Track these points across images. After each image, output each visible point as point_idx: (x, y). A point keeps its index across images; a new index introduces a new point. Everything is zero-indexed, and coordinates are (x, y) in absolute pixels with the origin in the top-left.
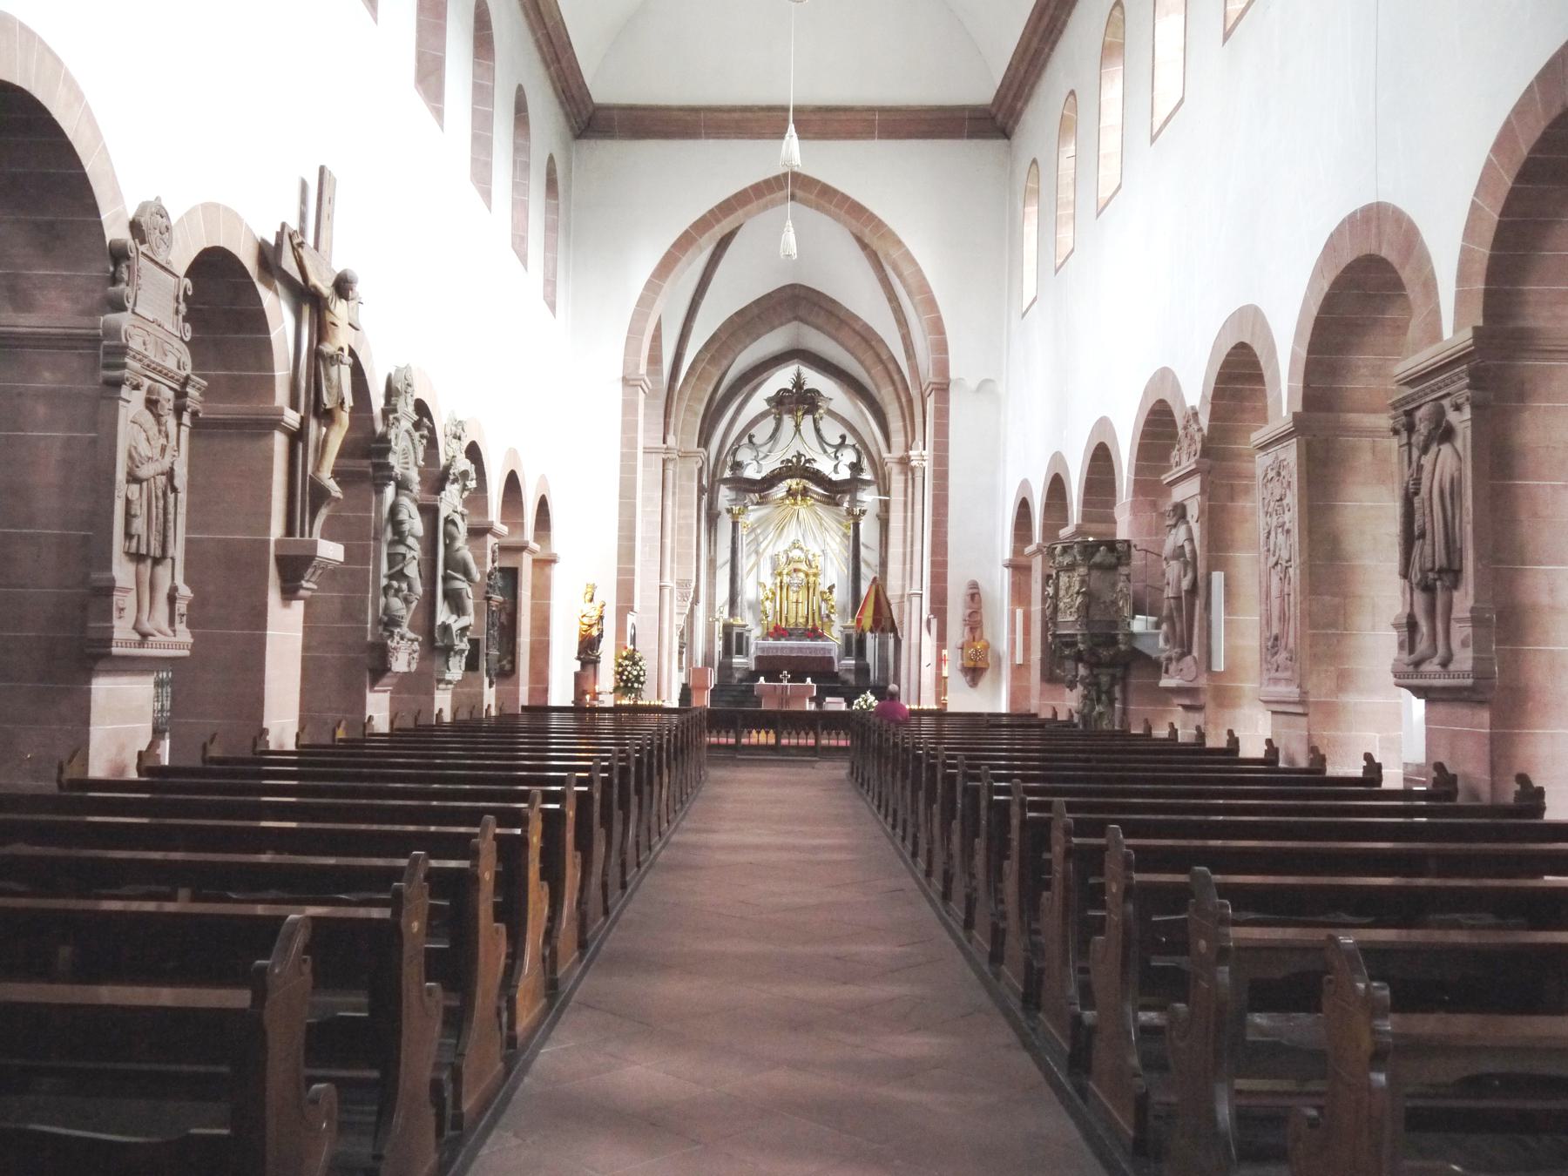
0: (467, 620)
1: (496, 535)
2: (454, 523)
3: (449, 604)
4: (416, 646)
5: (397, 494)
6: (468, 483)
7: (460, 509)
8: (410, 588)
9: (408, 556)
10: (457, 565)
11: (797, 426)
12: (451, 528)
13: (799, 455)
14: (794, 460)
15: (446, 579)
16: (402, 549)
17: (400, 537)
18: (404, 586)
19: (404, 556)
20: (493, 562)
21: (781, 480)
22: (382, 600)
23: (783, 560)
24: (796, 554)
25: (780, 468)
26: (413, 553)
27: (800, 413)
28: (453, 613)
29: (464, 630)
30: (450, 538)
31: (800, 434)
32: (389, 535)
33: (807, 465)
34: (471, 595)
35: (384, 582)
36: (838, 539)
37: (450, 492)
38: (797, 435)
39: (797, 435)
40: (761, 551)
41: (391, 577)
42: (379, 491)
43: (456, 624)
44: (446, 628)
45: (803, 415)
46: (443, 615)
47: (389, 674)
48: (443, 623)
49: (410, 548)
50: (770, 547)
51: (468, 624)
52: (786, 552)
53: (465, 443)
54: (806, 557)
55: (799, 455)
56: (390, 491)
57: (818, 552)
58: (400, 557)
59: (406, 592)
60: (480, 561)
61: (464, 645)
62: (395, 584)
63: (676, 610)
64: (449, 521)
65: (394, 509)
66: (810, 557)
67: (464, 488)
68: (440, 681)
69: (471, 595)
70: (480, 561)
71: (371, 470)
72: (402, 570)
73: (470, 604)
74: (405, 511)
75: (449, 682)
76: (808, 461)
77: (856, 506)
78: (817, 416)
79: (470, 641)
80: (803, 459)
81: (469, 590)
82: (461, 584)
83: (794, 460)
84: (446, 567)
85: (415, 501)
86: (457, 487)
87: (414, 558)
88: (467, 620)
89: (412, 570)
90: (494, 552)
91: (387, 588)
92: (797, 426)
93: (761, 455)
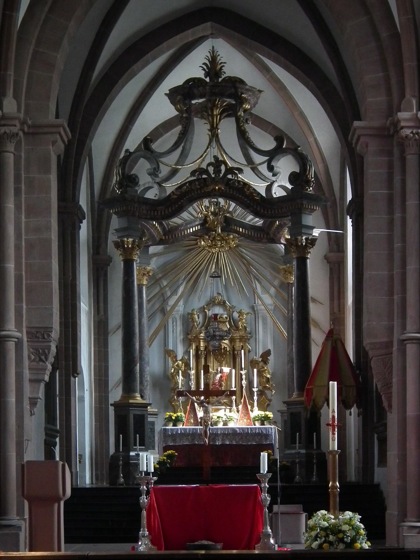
11: (213, 130)
13: (217, 163)
14: (211, 169)
21: (191, 201)
23: (199, 319)
24: (218, 310)
25: (190, 182)
27: (216, 112)
31: (218, 141)
33: (230, 176)
36: (272, 290)
38: (214, 144)
39: (214, 144)
40: (169, 308)
45: (221, 114)
50: (181, 303)
52: (202, 310)
54: (230, 316)
55: (217, 163)
57: (246, 310)
63: (27, 374)
66: (236, 315)
76: (230, 170)
77: (301, 234)
78: (241, 113)
80: (223, 168)
83: (211, 169)
92: (213, 130)
93: (164, 171)
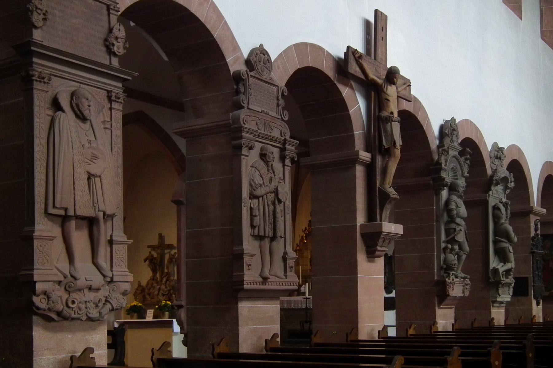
0: (511, 265)
1: (536, 214)
2: (499, 209)
3: (499, 257)
4: (468, 281)
5: (450, 194)
6: (509, 185)
7: (504, 200)
8: (461, 248)
9: (458, 229)
10: (501, 233)
12: (497, 212)
15: (495, 242)
16: (453, 226)
17: (452, 219)
18: (456, 247)
19: (455, 229)
20: (536, 230)
22: (443, 256)
26: (460, 227)
28: (501, 262)
29: (508, 272)
30: (497, 219)
32: (445, 217)
34: (511, 251)
35: (443, 245)
37: (496, 191)
41: (448, 242)
42: (438, 194)
43: (502, 268)
44: (496, 271)
46: (494, 263)
47: (448, 298)
48: (494, 268)
49: (458, 225)
51: (510, 267)
53: (506, 162)
56: (445, 193)
58: (452, 231)
59: (457, 250)
60: (522, 231)
61: (511, 280)
62: (450, 246)
64: (496, 208)
65: (448, 202)
67: (506, 188)
68: (494, 302)
69: (511, 251)
70: (522, 231)
71: (431, 182)
72: (454, 237)
73: (512, 256)
74: (454, 204)
75: (501, 303)
79: (515, 278)
81: (511, 248)
82: (506, 245)
84: (496, 234)
85: (460, 197)
86: (500, 188)
87: (461, 230)
88: (511, 265)
89: (461, 237)
90: (536, 225)
91: (445, 249)
